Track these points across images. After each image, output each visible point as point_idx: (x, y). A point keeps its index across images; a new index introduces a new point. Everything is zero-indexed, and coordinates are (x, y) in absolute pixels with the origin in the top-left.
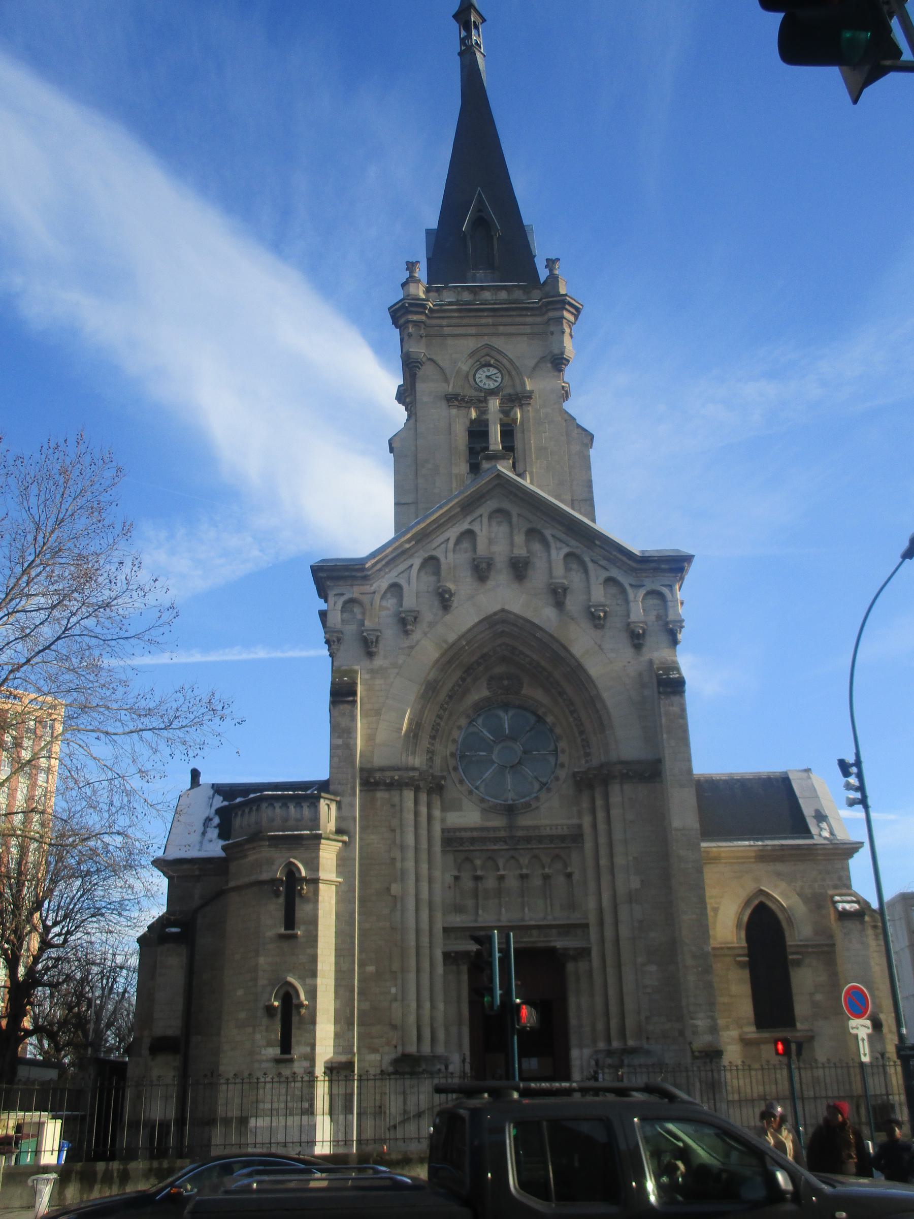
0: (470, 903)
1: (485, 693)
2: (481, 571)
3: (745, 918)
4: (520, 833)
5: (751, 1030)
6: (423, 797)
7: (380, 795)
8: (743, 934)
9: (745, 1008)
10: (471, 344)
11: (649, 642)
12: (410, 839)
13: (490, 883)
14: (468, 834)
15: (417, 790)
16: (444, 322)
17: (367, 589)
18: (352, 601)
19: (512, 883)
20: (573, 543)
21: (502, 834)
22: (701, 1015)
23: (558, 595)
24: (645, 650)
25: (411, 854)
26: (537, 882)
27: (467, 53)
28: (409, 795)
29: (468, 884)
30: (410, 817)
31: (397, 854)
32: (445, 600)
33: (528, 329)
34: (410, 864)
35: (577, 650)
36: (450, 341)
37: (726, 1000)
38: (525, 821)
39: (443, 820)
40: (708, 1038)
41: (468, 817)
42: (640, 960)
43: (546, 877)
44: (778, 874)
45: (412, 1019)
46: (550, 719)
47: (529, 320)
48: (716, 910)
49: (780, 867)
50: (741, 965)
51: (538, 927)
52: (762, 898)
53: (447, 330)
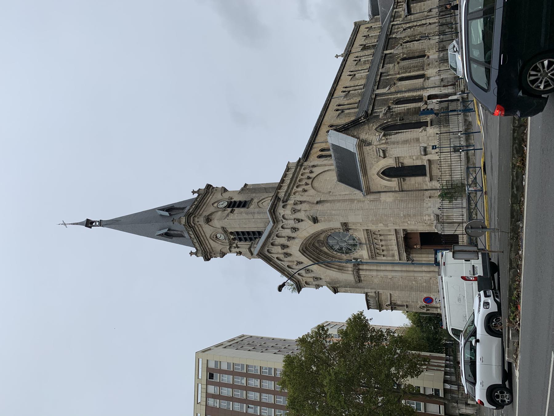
0: (391, 252)
1: (324, 248)
2: (287, 255)
3: (388, 178)
4: (368, 242)
5: (427, 178)
6: (361, 267)
7: (362, 279)
8: (393, 179)
9: (419, 179)
10: (211, 241)
11: (300, 218)
12: (374, 273)
13: (384, 248)
14: (370, 253)
15: (359, 269)
16: (207, 248)
17: (301, 280)
18: (306, 282)
19: (383, 243)
20: (273, 235)
21: (368, 246)
22: (425, 218)
23: (289, 238)
24: (303, 219)
25: (379, 273)
26: (382, 238)
27: (101, 223)
28: (361, 273)
29: (385, 253)
30: (368, 273)
31: (379, 276)
32: (299, 263)
33: (200, 228)
34: (382, 274)
35: (308, 235)
36: (212, 246)
37: (417, 185)
38: (363, 241)
39: (367, 259)
40: (432, 217)
41: (363, 253)
42: (407, 224)
43: (380, 235)
44: (371, 168)
45: (428, 275)
46: (329, 234)
47: (197, 229)
48: (385, 186)
49: (368, 168)
50: (404, 180)
51: (397, 239)
52: (380, 173)
53: (209, 247)
